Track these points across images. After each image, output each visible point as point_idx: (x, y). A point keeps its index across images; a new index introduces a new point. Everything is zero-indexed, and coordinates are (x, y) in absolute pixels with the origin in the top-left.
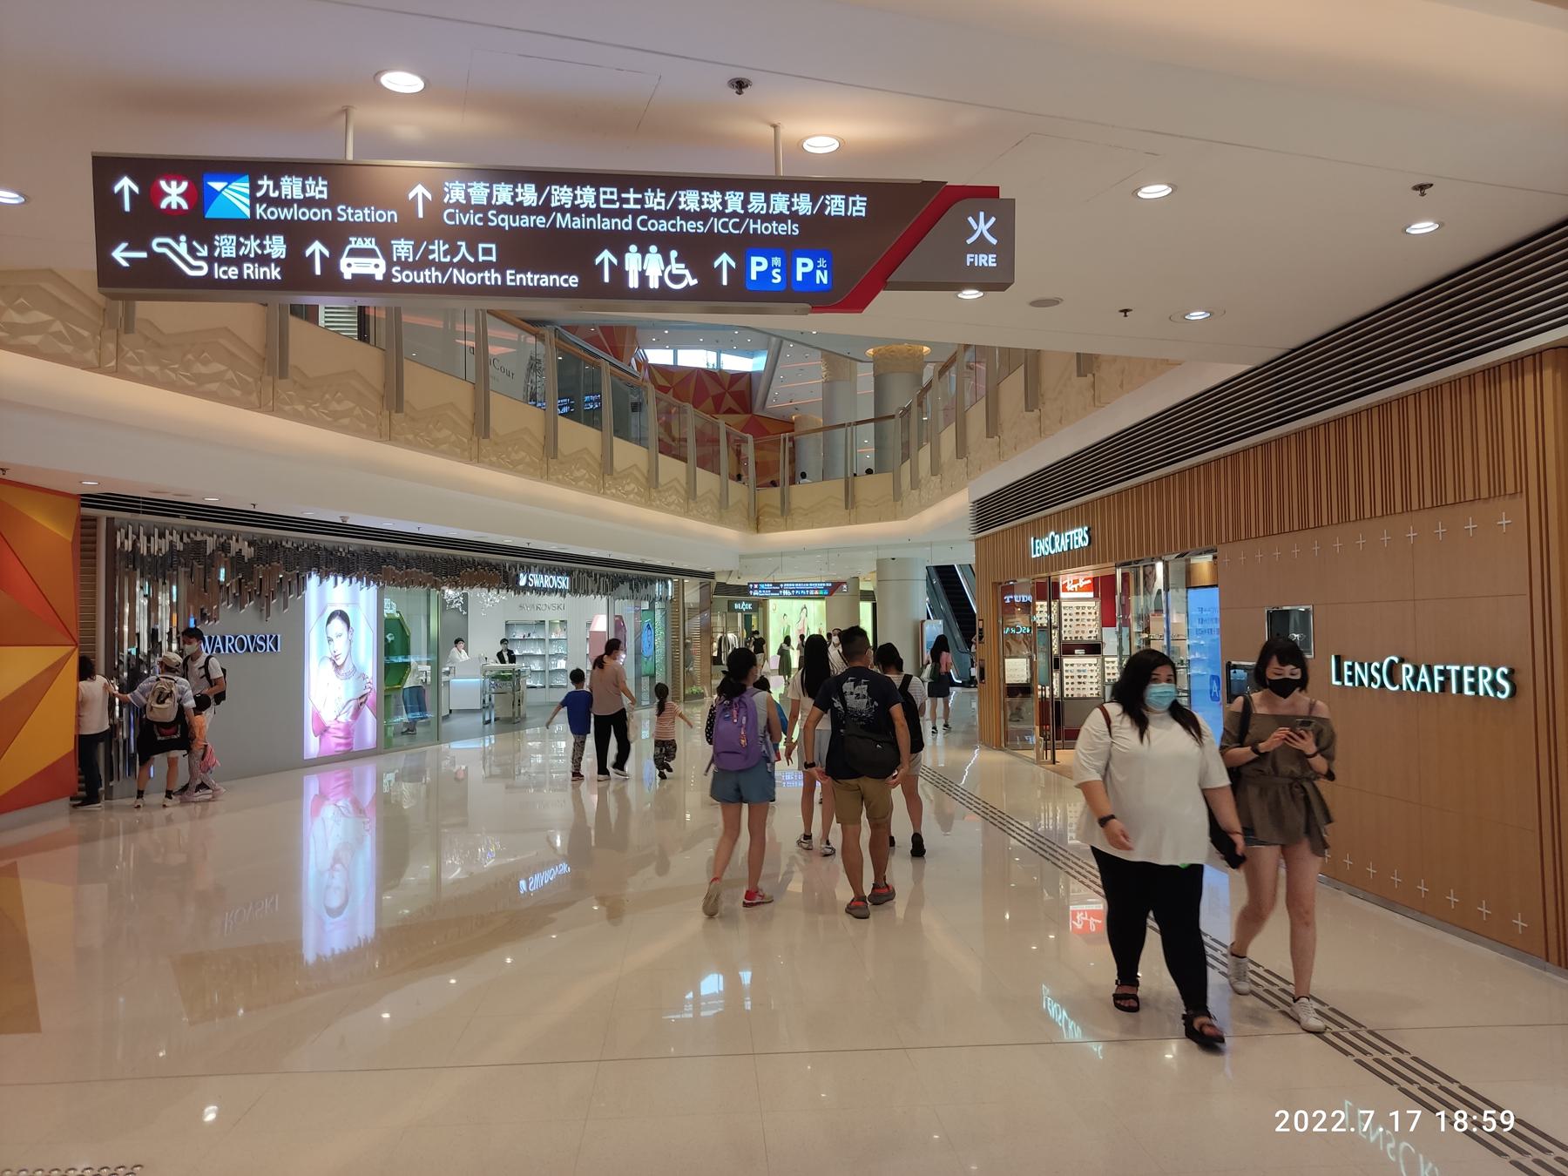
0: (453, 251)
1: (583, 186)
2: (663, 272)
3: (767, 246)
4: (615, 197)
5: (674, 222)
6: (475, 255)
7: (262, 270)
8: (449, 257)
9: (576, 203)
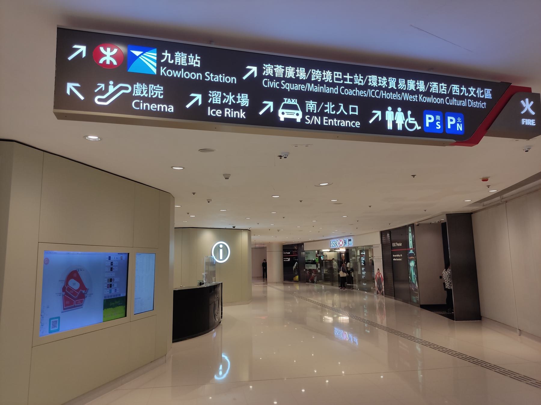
0: (337, 108)
1: (326, 70)
2: (404, 122)
3: (433, 108)
4: (341, 77)
5: (355, 90)
6: (347, 111)
7: (235, 113)
8: (335, 111)
9: (323, 79)
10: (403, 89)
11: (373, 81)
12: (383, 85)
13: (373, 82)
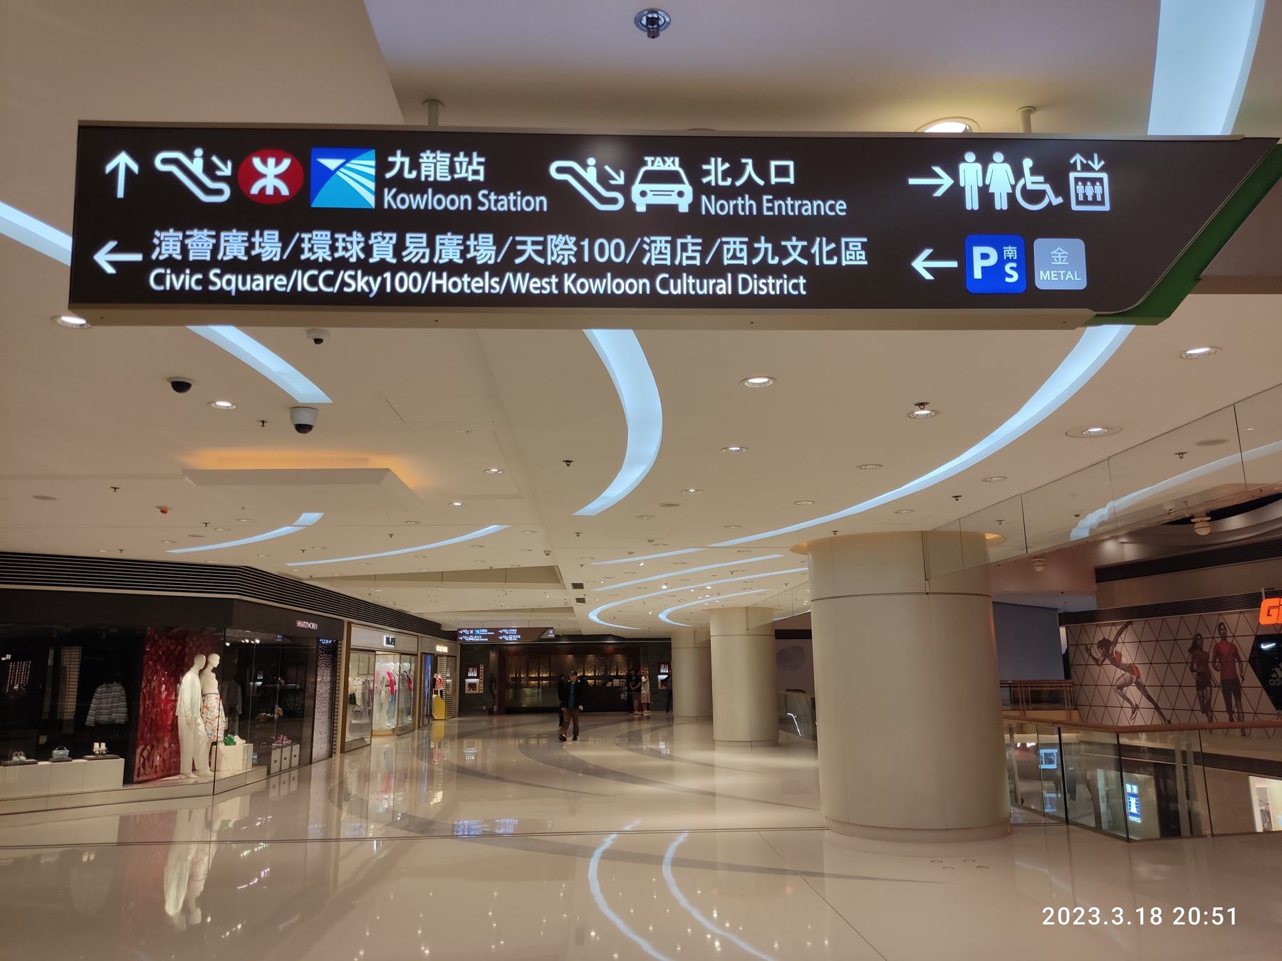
10: (419, 261)
11: (315, 246)
12: (351, 256)
13: (318, 248)
